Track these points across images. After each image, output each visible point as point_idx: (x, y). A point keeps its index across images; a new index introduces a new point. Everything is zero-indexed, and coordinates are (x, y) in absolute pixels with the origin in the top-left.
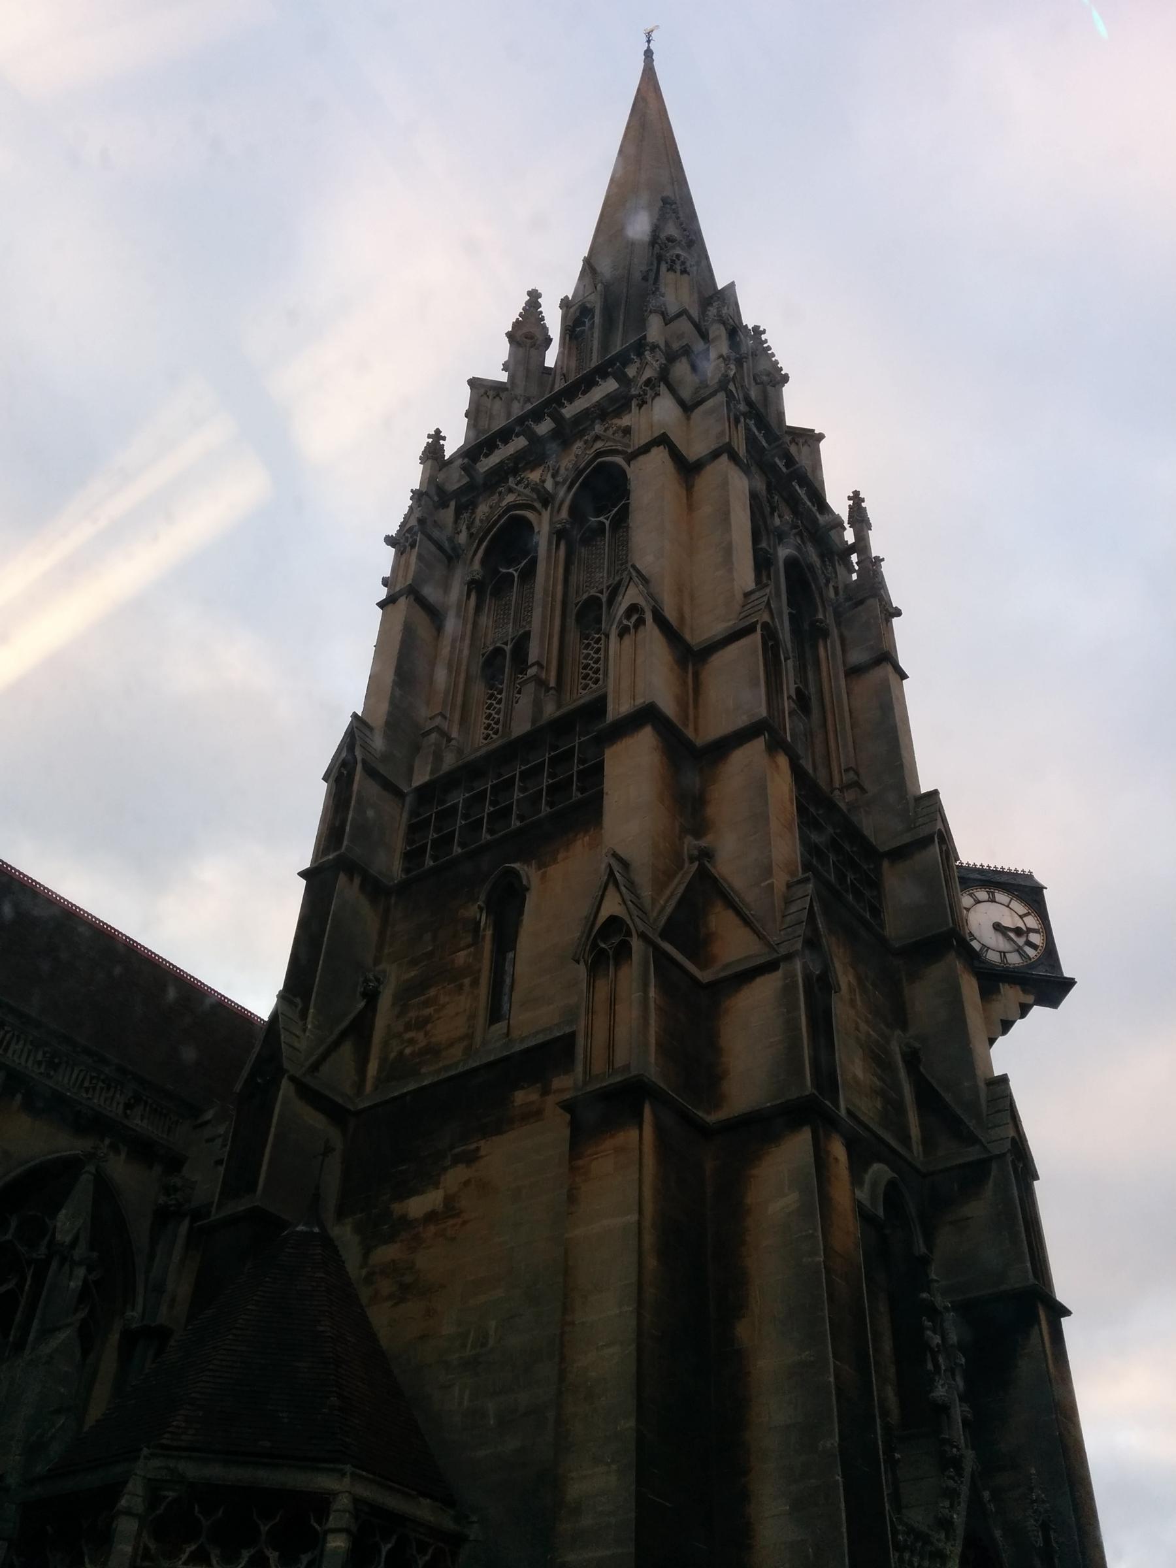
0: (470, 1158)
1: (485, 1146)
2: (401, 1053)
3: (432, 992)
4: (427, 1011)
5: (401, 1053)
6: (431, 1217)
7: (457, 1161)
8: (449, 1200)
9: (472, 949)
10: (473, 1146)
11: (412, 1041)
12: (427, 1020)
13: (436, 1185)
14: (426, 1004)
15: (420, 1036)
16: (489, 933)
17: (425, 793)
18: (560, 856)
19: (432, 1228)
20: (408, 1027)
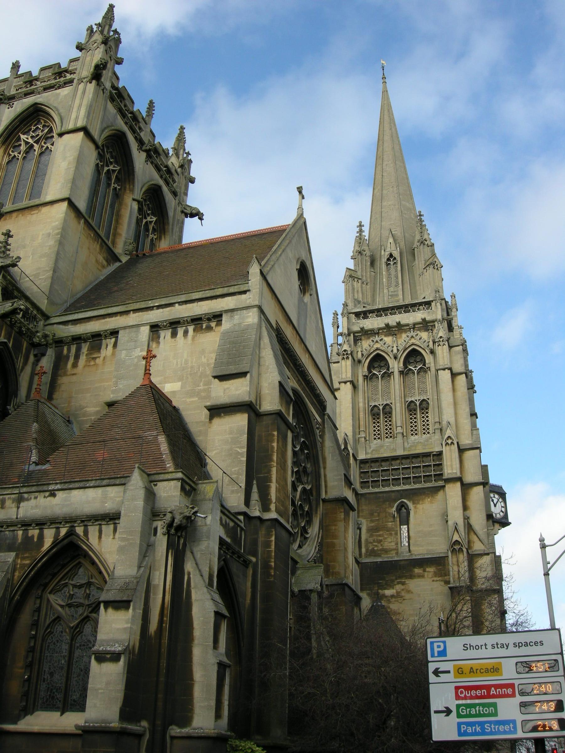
0: (403, 584)
1: (407, 581)
2: (373, 548)
3: (381, 533)
4: (380, 538)
5: (373, 548)
6: (392, 596)
7: (398, 583)
8: (398, 593)
9: (393, 523)
10: (403, 581)
11: (376, 546)
12: (381, 541)
13: (393, 588)
14: (380, 536)
15: (379, 545)
16: (398, 519)
17: (364, 462)
18: (421, 502)
19: (394, 599)
20: (374, 541)
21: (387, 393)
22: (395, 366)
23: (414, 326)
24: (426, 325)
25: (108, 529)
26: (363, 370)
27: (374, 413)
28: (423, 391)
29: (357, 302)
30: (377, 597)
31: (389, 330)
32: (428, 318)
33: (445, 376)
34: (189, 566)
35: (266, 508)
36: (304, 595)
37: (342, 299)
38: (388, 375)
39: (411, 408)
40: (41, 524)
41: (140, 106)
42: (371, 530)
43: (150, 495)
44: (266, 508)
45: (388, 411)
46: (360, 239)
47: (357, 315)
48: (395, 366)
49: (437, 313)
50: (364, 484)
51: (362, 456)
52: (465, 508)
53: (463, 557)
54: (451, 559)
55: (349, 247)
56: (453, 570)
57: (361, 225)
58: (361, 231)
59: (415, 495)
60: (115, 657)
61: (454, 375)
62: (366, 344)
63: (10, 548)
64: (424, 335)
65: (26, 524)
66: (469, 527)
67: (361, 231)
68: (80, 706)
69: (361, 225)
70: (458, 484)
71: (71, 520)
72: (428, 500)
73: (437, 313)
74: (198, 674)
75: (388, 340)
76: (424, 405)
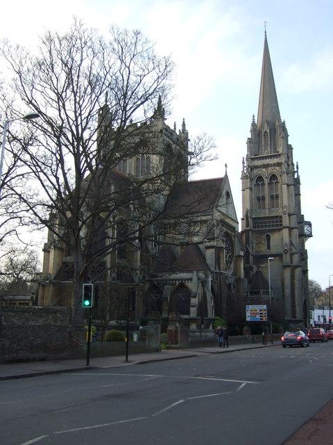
21: (263, 190)
22: (266, 181)
23: (274, 165)
24: (279, 164)
25: (189, 282)
26: (254, 182)
27: (258, 199)
28: (277, 190)
29: (251, 152)
30: (258, 267)
31: (266, 166)
32: (280, 161)
33: (285, 187)
34: (206, 289)
35: (220, 270)
36: (230, 284)
37: (246, 153)
38: (263, 184)
39: (272, 197)
40: (176, 280)
41: (172, 128)
42: (257, 244)
43: (197, 275)
44: (220, 270)
45: (263, 198)
46: (253, 124)
47: (252, 159)
48: (266, 181)
49: (283, 159)
50: (254, 227)
51: (254, 217)
52: (290, 236)
53: (288, 255)
54: (284, 256)
55: (249, 127)
56: (284, 260)
57: (254, 117)
58: (254, 119)
59: (273, 231)
60: (194, 306)
61: (288, 185)
62: (255, 171)
63: (170, 285)
64: (278, 168)
65: (172, 280)
66: (291, 243)
67: (254, 119)
68: (188, 313)
69: (254, 117)
70: (287, 229)
71: (182, 279)
72: (277, 234)
73: (283, 159)
74: (209, 308)
75: (264, 170)
76: (277, 197)
